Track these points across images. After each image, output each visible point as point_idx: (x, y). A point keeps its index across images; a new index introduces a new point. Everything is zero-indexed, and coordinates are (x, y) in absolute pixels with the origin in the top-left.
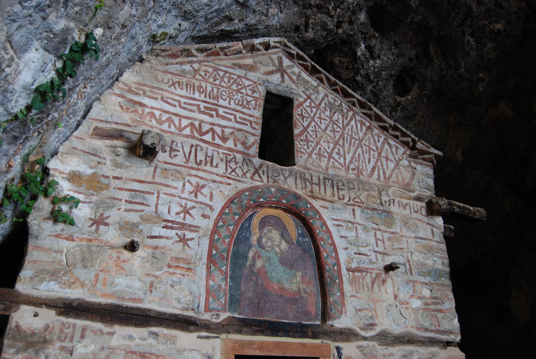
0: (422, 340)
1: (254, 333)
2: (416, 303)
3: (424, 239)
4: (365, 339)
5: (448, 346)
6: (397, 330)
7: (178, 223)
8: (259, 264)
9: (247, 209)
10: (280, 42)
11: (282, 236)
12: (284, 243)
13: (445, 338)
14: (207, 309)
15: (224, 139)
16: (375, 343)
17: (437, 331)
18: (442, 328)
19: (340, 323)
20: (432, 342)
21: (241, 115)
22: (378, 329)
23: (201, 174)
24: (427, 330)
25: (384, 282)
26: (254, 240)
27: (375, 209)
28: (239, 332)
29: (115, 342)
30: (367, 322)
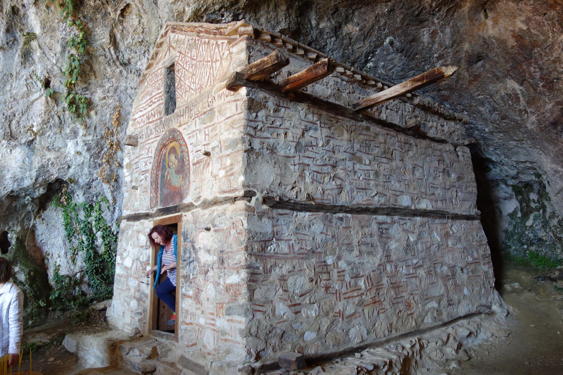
0: (221, 200)
1: (162, 215)
2: (222, 173)
3: (230, 117)
4: (196, 207)
5: (235, 201)
6: (210, 197)
7: (145, 171)
8: (168, 178)
9: (161, 150)
10: (167, 26)
11: (176, 157)
12: (176, 161)
13: (232, 195)
14: (151, 208)
15: (154, 116)
16: (199, 209)
17: (230, 192)
18: (232, 188)
19: (186, 201)
20: (227, 200)
21: (158, 96)
22: (202, 199)
23: (150, 141)
24: (224, 192)
25: (208, 164)
26: (167, 165)
27: (205, 113)
28: (158, 216)
29: (135, 228)
30: (198, 196)
